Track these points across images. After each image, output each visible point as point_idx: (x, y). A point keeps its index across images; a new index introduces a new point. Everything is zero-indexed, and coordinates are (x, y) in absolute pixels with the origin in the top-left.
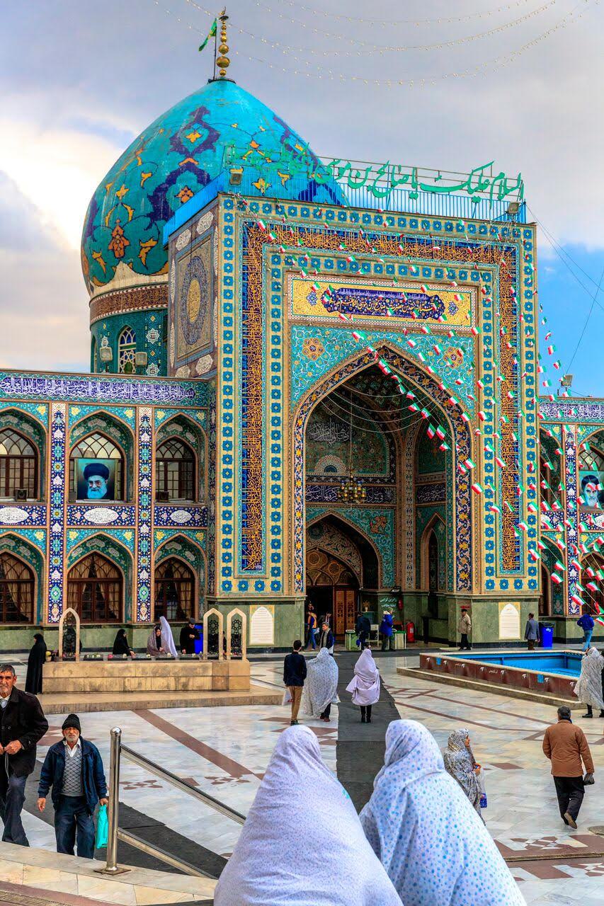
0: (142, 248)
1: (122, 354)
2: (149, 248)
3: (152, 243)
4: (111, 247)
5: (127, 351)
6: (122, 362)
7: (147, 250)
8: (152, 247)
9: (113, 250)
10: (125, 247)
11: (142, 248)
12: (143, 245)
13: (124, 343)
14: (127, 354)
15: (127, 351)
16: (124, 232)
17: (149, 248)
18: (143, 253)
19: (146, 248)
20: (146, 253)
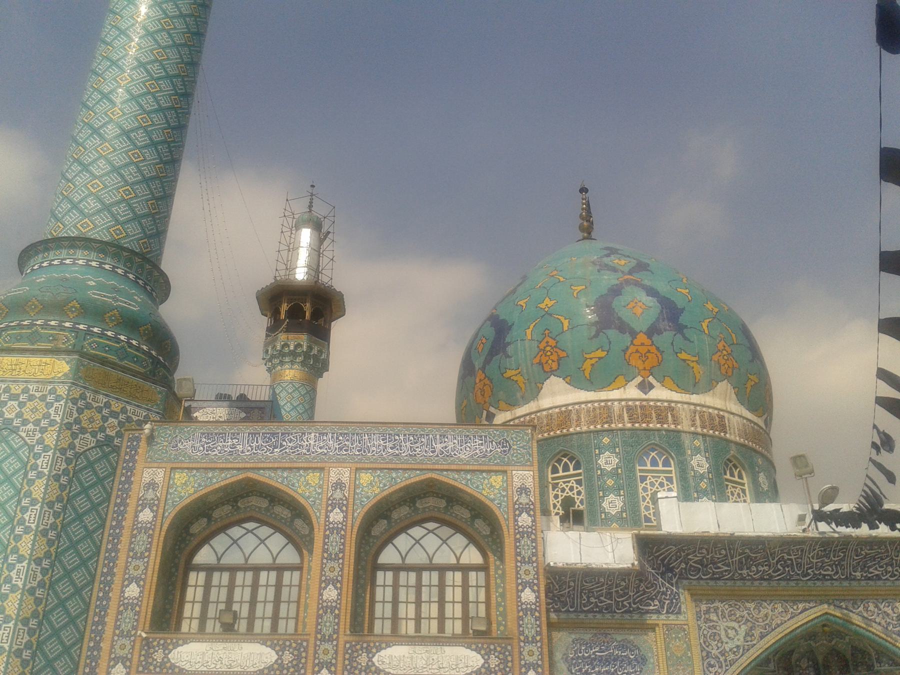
0: (586, 359)
1: (555, 486)
2: (597, 360)
3: (600, 354)
4: (537, 360)
5: (564, 482)
6: (556, 497)
7: (593, 361)
8: (600, 358)
9: (540, 363)
10: (559, 359)
11: (586, 359)
12: (587, 356)
13: (569, 470)
14: (564, 486)
15: (564, 482)
16: (556, 343)
17: (597, 360)
18: (587, 365)
19: (591, 359)
20: (593, 365)
